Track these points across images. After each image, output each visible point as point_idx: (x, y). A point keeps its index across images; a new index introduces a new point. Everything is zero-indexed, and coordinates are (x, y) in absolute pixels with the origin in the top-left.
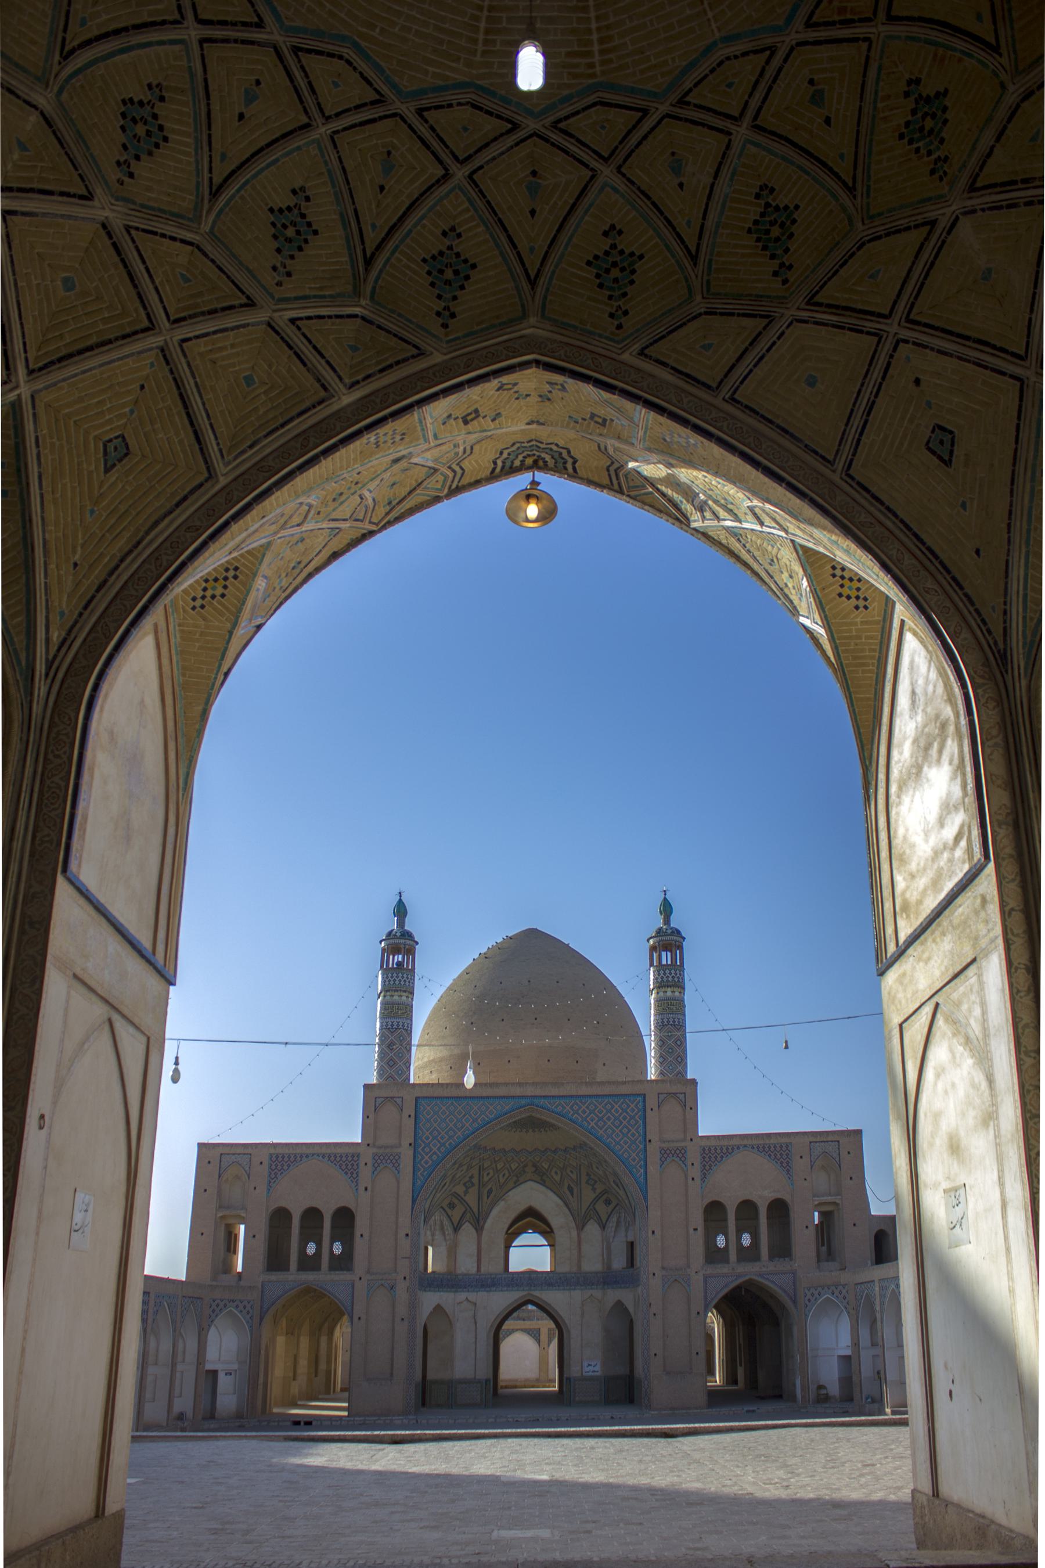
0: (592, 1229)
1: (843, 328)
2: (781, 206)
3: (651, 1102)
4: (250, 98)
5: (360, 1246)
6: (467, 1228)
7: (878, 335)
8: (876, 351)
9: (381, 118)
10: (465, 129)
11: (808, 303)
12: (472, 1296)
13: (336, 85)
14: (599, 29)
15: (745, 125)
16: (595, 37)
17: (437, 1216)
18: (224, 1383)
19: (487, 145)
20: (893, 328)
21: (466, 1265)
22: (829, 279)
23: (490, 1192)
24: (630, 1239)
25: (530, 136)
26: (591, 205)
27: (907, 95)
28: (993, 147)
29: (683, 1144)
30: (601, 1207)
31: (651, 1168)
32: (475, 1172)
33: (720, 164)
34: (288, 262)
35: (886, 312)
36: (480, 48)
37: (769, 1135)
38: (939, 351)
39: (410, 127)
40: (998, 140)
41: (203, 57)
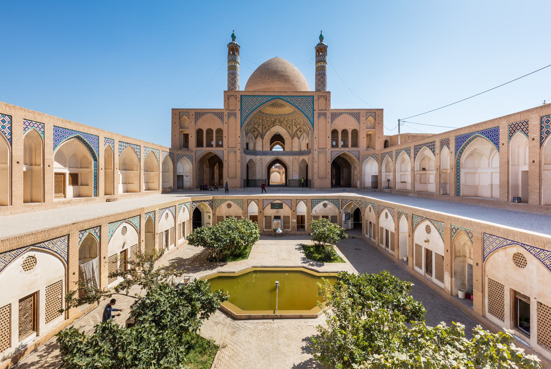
0: (296, 139)
3: (316, 98)
5: (225, 140)
6: (259, 138)
12: (261, 157)
17: (250, 135)
18: (185, 178)
21: (259, 148)
23: (265, 127)
24: (307, 142)
29: (325, 111)
30: (298, 133)
31: (315, 118)
32: (261, 121)
37: (353, 110)
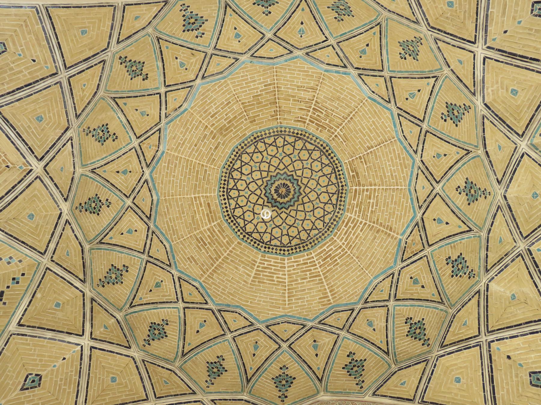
1: (461, 350)
2: (417, 322)
4: (201, 326)
7: (478, 345)
8: (481, 352)
9: (252, 331)
10: (285, 331)
11: (441, 347)
13: (235, 321)
14: (329, 288)
15: (392, 300)
16: (328, 291)
19: (294, 334)
20: (483, 338)
22: (446, 335)
25: (311, 328)
26: (340, 346)
27: (448, 264)
28: (487, 254)
33: (387, 317)
34: (213, 380)
35: (477, 334)
36: (287, 303)
38: (511, 338)
39: (264, 332)
40: (487, 250)
41: (184, 313)
